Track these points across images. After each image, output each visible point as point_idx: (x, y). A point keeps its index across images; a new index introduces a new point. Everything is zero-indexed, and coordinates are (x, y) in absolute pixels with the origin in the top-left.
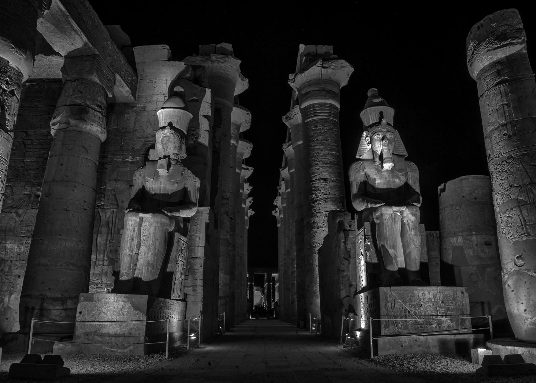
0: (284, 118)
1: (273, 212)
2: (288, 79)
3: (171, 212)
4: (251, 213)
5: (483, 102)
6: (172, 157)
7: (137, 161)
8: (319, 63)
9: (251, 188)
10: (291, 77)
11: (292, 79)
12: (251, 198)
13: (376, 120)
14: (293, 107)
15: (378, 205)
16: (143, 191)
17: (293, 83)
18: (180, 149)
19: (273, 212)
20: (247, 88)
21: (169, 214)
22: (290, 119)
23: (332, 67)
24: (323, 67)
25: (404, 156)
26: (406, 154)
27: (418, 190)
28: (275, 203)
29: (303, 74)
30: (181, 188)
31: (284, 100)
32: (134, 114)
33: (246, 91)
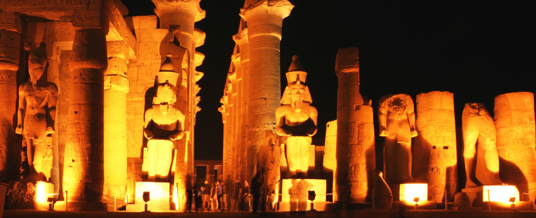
0: (234, 38)
1: (219, 109)
2: (239, 12)
3: (173, 138)
4: (198, 109)
5: (338, 90)
6: (169, 103)
7: (141, 101)
8: (266, 3)
9: (200, 89)
10: (242, 11)
11: (243, 12)
12: (199, 97)
13: (295, 80)
14: (243, 29)
15: (288, 135)
16: (152, 123)
17: (244, 15)
18: (173, 98)
19: (219, 109)
20: (204, 17)
21: (173, 140)
22: (240, 38)
23: (277, 5)
24: (269, 5)
25: (309, 102)
26: (311, 101)
27: (316, 124)
28: (222, 101)
29: (252, 10)
30: (174, 121)
31: (234, 25)
32: (136, 67)
33: (203, 20)
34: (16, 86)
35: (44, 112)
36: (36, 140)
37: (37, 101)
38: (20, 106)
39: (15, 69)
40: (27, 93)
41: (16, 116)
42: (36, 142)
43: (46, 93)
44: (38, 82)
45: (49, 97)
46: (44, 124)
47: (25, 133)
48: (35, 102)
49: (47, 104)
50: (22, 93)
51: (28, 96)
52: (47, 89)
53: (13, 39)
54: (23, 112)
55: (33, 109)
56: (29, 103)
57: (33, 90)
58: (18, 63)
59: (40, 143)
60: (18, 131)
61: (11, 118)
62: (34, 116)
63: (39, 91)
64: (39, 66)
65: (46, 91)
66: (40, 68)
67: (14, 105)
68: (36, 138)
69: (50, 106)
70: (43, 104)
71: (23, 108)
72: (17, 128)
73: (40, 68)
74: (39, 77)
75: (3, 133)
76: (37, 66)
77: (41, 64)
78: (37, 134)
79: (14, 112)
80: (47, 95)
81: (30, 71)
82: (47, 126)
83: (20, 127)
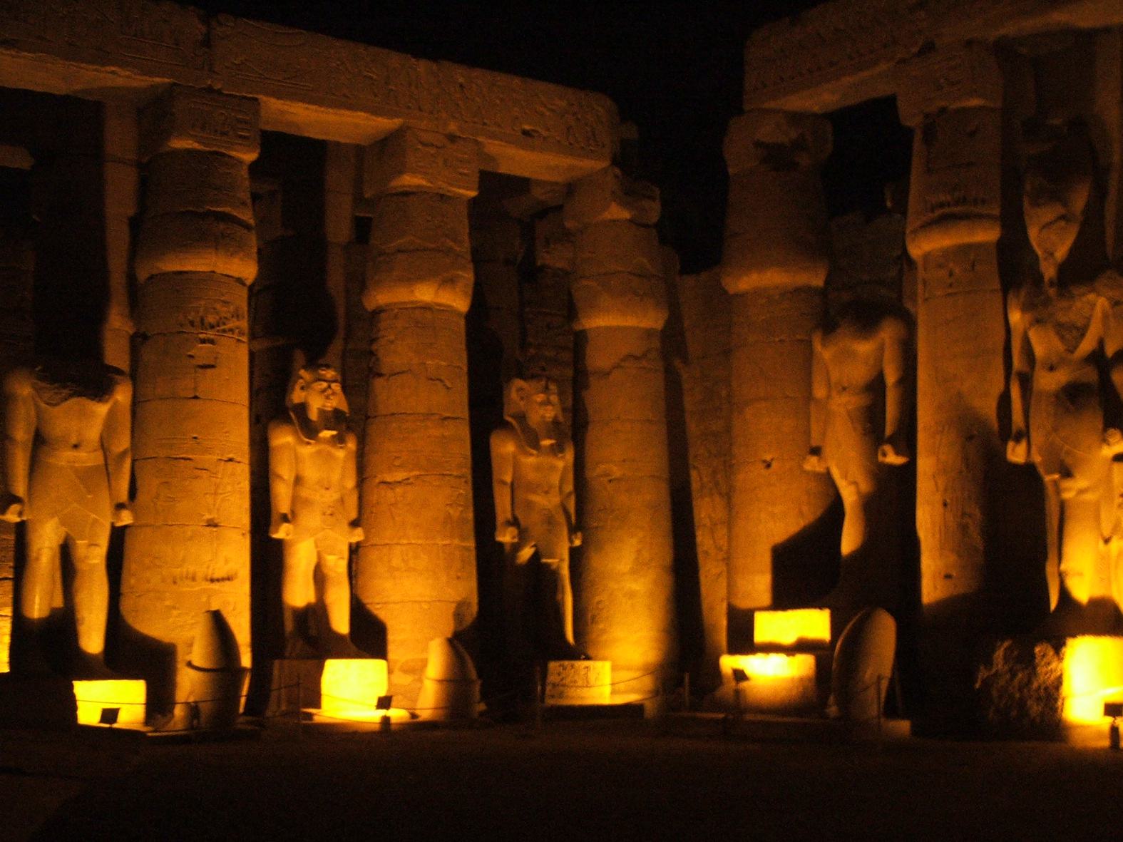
34: (1000, 294)
35: (1091, 375)
36: (1066, 484)
37: (1062, 338)
38: (1017, 363)
39: (987, 234)
40: (1028, 317)
41: (1005, 400)
42: (1071, 490)
43: (1093, 306)
44: (1063, 268)
45: (1105, 316)
46: (1094, 419)
47: (1037, 459)
48: (1059, 346)
49: (1101, 343)
50: (1016, 317)
51: (1031, 325)
52: (1093, 290)
53: (972, 134)
54: (1026, 382)
55: (1052, 369)
56: (1039, 350)
57: (1047, 302)
58: (996, 211)
59: (1081, 492)
60: (1017, 454)
61: (988, 408)
62: (1057, 396)
63: (1065, 304)
64: (1058, 210)
65: (1091, 297)
66: (1063, 217)
67: (999, 362)
68: (1067, 473)
69: (1110, 350)
70: (1087, 346)
71: (1026, 369)
72: (1011, 444)
73: (1063, 217)
74: (1061, 253)
75: (967, 466)
76: (1049, 213)
77: (1065, 204)
78: (1068, 460)
79: (998, 387)
80: (1098, 309)
81: (1033, 233)
82: (1105, 429)
83: (1018, 439)
